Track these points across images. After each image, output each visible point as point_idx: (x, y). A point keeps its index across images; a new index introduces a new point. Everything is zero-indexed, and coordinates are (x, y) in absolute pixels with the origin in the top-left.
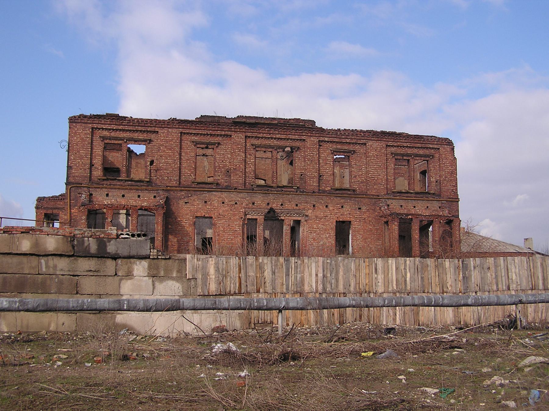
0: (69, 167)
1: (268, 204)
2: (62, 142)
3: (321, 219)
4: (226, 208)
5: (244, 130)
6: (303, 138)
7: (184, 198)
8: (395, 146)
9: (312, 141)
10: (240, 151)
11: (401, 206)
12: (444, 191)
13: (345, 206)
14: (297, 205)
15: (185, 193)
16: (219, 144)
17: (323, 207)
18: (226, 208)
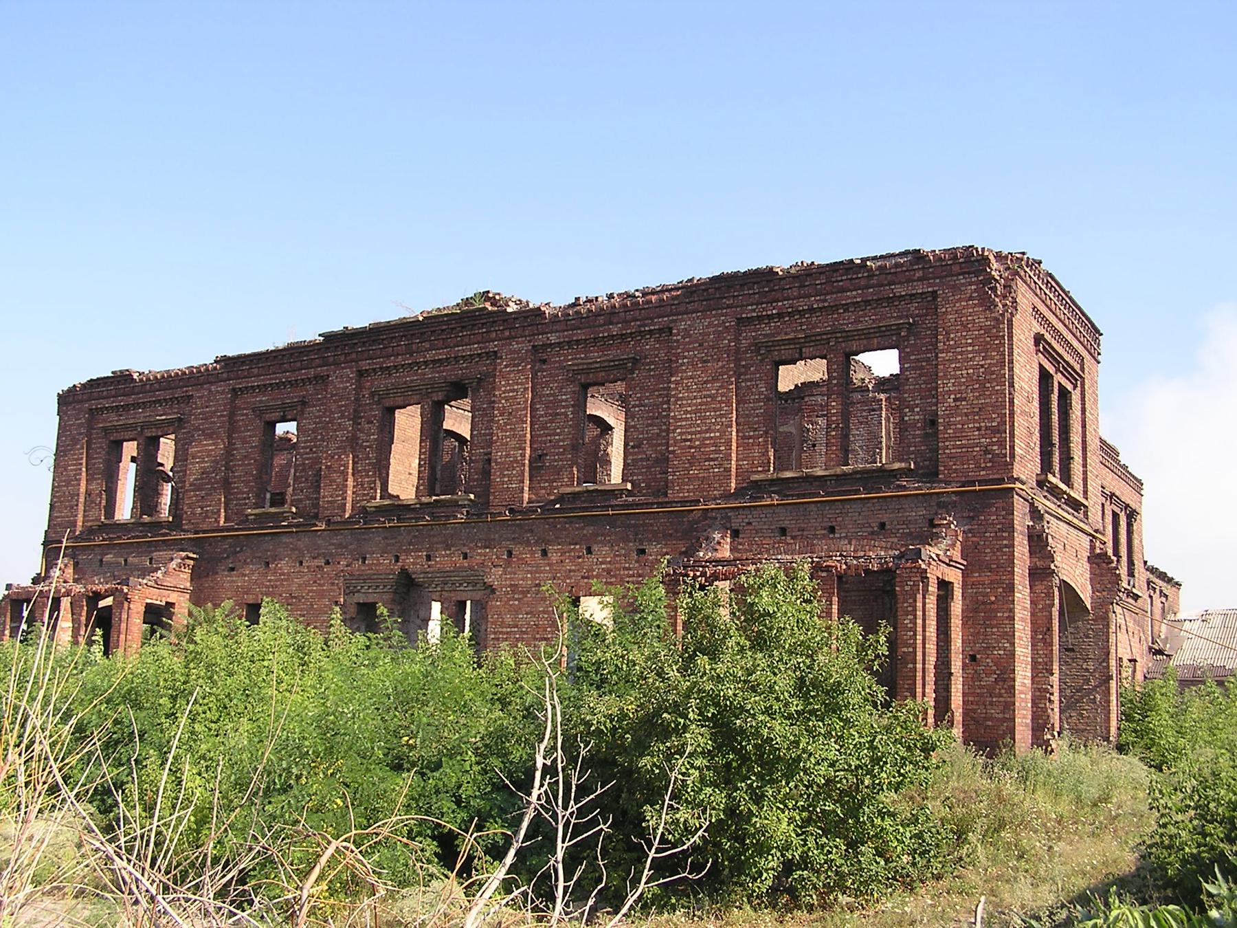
0: (52, 506)
1: (397, 559)
2: (34, 449)
3: (525, 593)
4: (306, 578)
5: (354, 356)
6: (492, 347)
7: (228, 557)
8: (770, 317)
9: (514, 352)
10: (342, 417)
11: (783, 531)
12: (950, 457)
13: (595, 548)
14: (465, 557)
15: (230, 544)
16: (304, 403)
17: (532, 553)
18: (306, 578)
